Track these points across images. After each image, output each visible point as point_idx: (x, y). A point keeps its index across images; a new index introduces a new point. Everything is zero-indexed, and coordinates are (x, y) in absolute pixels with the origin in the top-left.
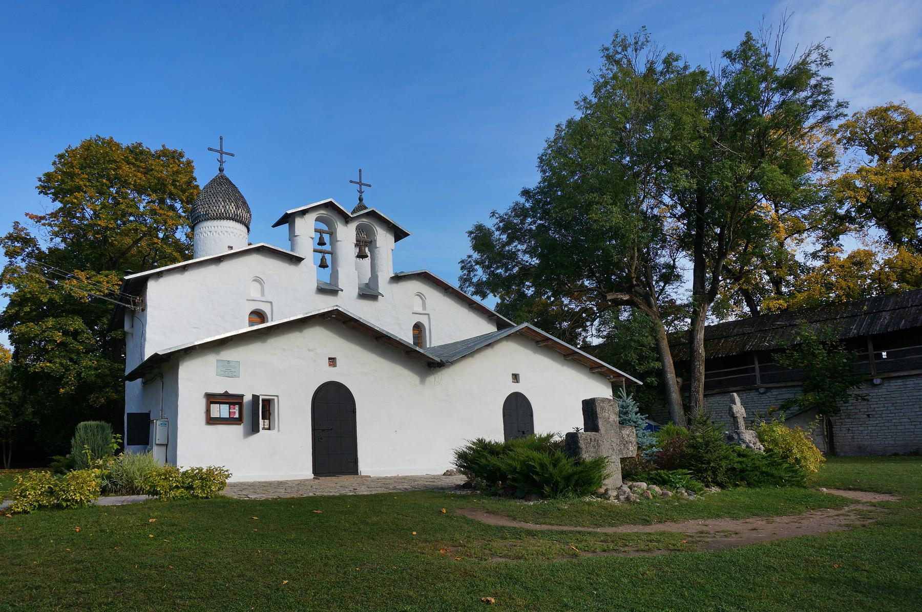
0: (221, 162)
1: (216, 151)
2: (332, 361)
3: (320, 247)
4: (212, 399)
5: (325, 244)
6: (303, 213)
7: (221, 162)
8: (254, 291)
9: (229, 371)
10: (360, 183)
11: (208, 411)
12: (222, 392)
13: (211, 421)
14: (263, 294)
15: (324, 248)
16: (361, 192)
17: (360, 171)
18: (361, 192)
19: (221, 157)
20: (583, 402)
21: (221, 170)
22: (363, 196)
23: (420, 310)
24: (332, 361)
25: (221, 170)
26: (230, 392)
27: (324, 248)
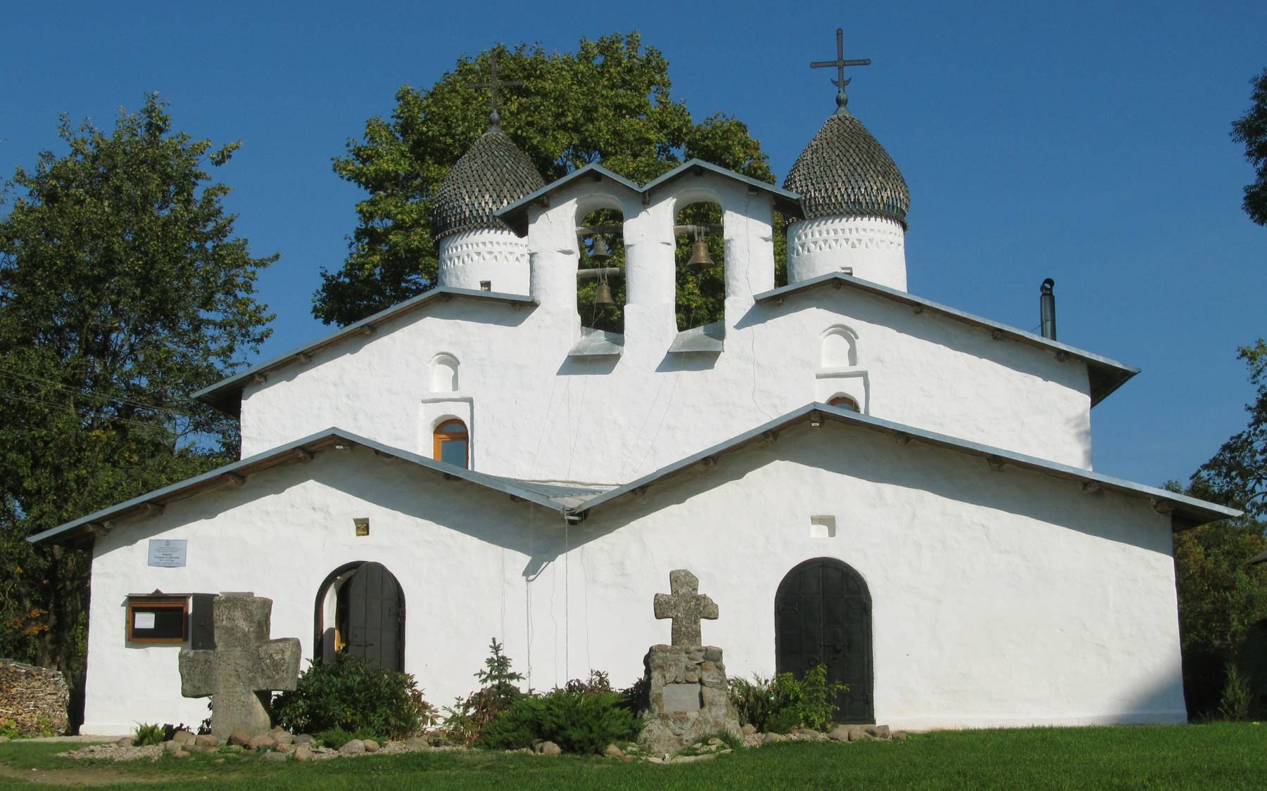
2: (363, 527)
4: (136, 604)
6: (543, 204)
8: (439, 380)
9: (169, 557)
10: (840, 64)
11: (131, 621)
12: (150, 591)
13: (137, 637)
14: (455, 387)
16: (841, 83)
17: (839, 33)
20: (266, 605)
23: (844, 366)
24: (363, 527)
26: (165, 591)
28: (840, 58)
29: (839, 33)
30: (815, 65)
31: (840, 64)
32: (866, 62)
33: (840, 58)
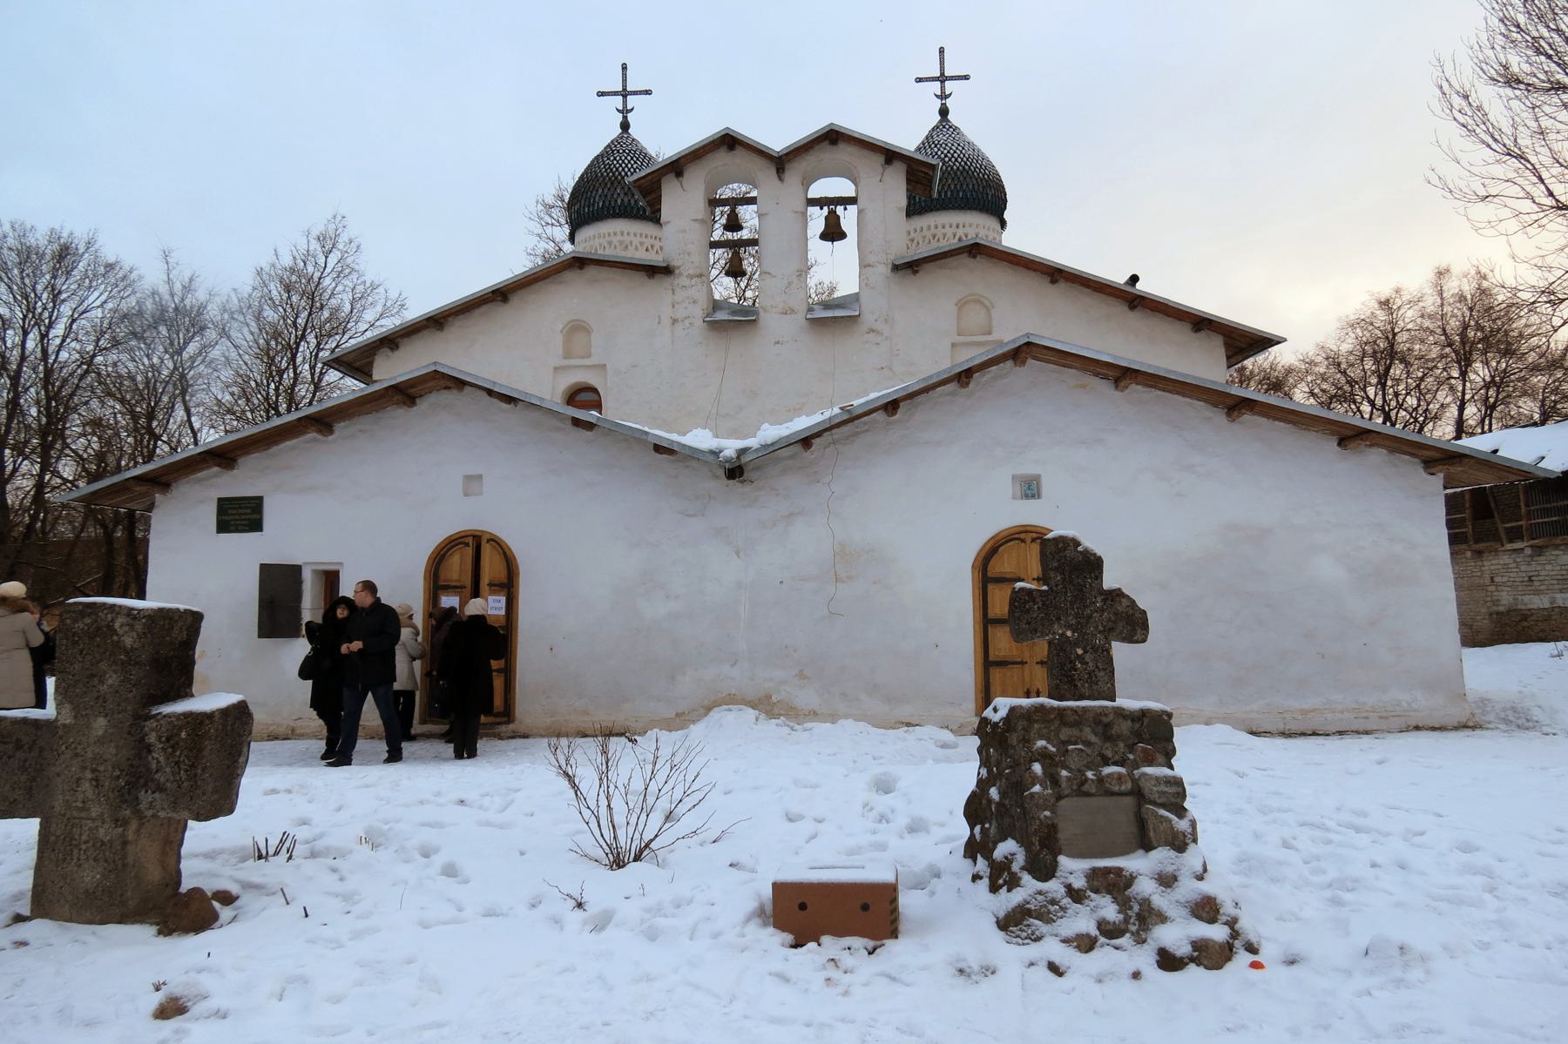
0: (625, 111)
1: (615, 93)
3: (729, 235)
5: (738, 227)
7: (625, 111)
10: (942, 79)
15: (736, 236)
16: (943, 96)
17: (942, 51)
18: (943, 96)
19: (625, 103)
21: (625, 126)
22: (949, 102)
24: (472, 483)
25: (625, 126)
27: (736, 236)
28: (942, 74)
29: (942, 51)
30: (919, 80)
31: (942, 79)
32: (966, 78)
33: (942, 74)
